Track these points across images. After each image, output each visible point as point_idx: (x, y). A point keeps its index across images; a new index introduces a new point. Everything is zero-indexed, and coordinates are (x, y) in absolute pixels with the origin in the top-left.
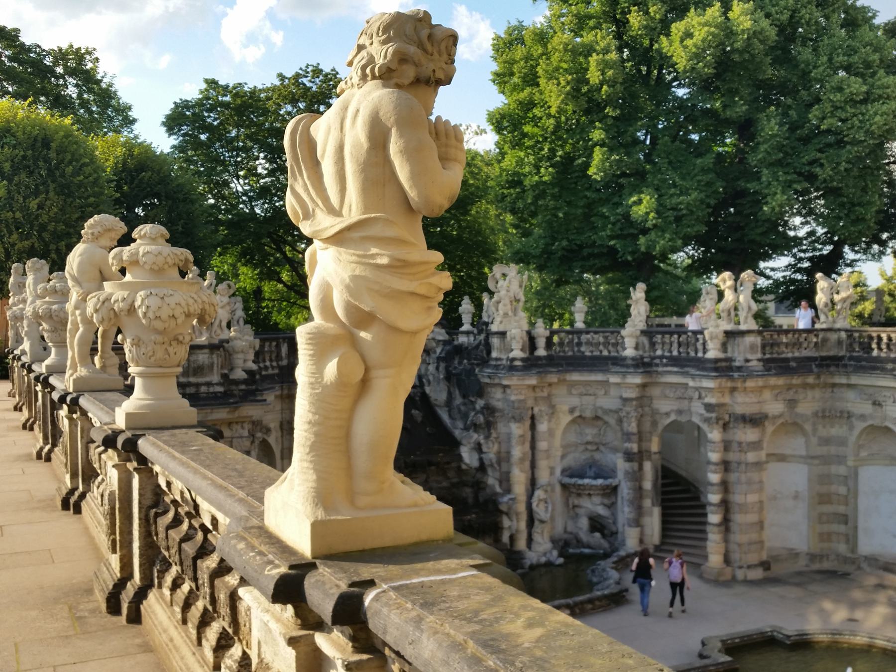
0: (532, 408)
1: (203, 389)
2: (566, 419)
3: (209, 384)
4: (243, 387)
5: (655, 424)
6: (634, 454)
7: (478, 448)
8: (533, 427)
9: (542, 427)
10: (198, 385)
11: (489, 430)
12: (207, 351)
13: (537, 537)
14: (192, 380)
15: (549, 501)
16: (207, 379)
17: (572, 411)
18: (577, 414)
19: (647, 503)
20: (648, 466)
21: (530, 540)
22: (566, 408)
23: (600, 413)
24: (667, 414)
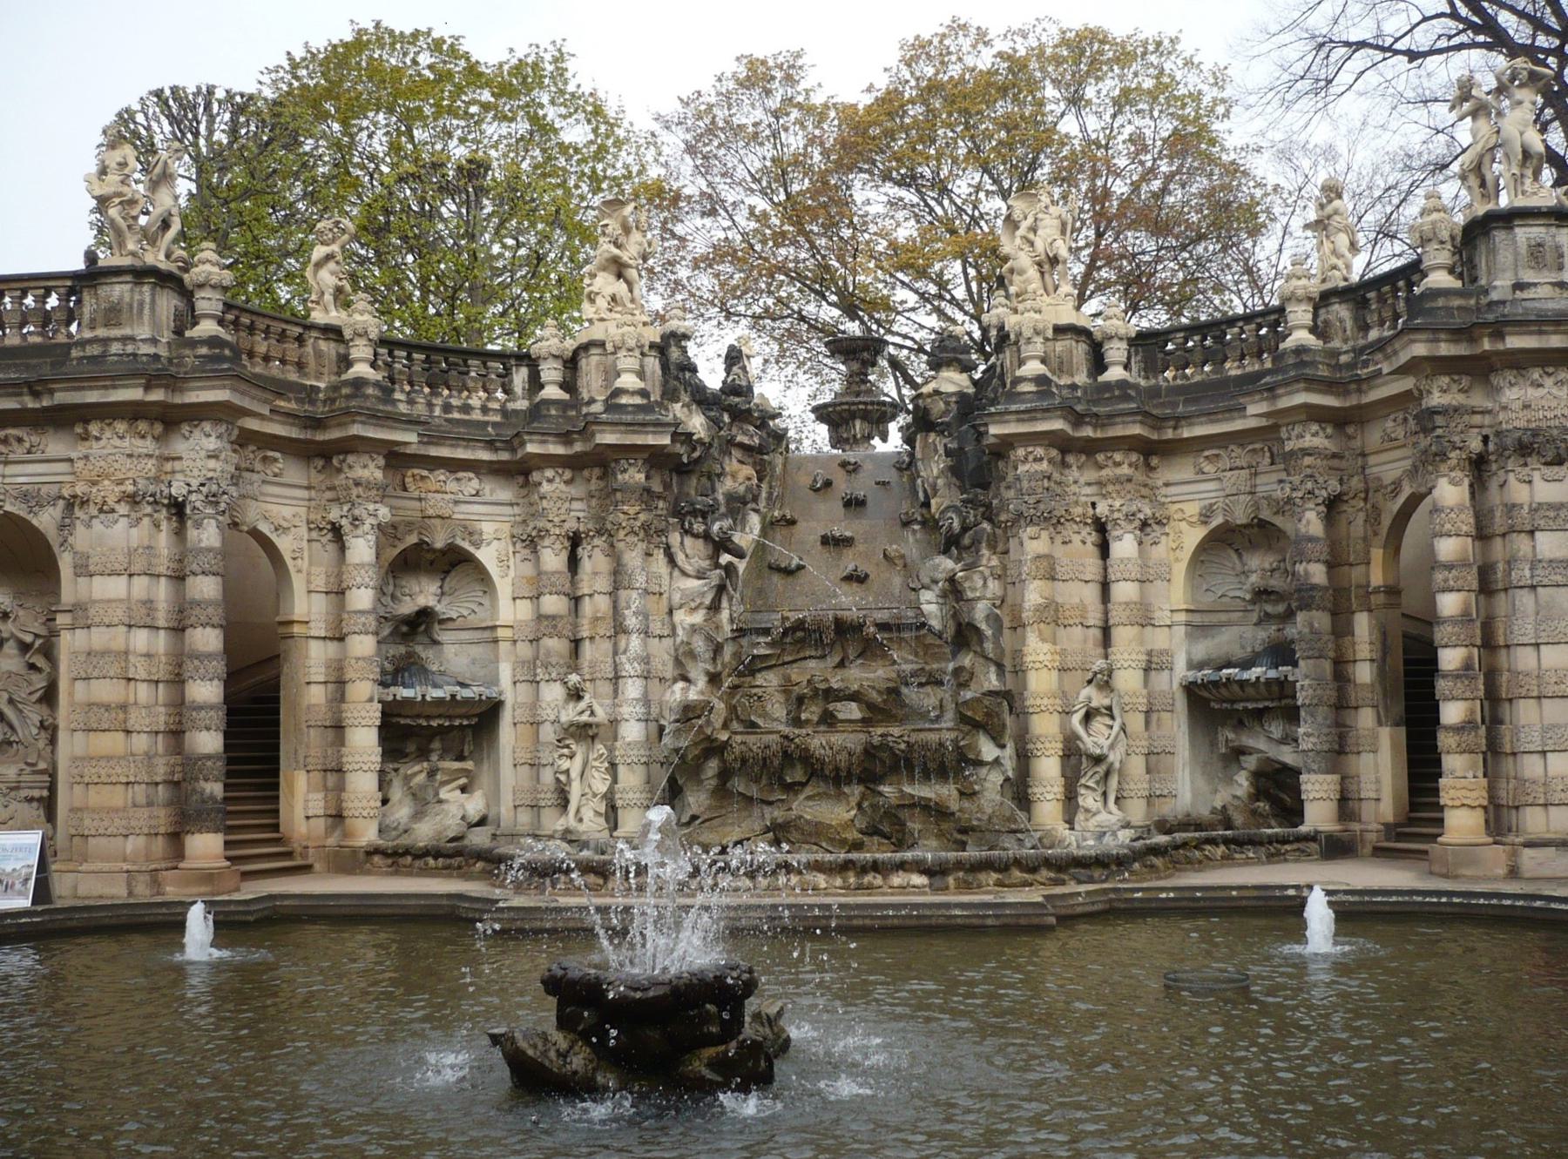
0: (1094, 505)
1: (115, 348)
2: (1193, 536)
3: (125, 340)
4: (204, 351)
5: (1374, 516)
6: (1314, 587)
7: (953, 590)
8: (1104, 549)
9: (1124, 546)
10: (106, 341)
11: (977, 551)
12: (128, 278)
13: (1088, 800)
14: (101, 332)
15: (1116, 712)
16: (127, 331)
17: (1205, 517)
18: (1217, 521)
19: (1366, 718)
20: (1363, 624)
21: (1070, 799)
22: (1193, 509)
23: (1266, 514)
24: (1397, 487)
